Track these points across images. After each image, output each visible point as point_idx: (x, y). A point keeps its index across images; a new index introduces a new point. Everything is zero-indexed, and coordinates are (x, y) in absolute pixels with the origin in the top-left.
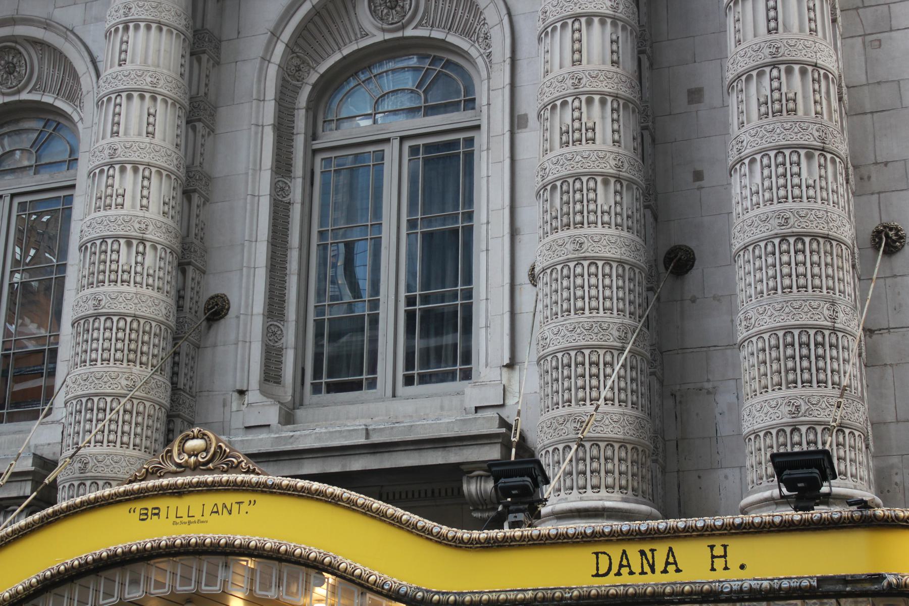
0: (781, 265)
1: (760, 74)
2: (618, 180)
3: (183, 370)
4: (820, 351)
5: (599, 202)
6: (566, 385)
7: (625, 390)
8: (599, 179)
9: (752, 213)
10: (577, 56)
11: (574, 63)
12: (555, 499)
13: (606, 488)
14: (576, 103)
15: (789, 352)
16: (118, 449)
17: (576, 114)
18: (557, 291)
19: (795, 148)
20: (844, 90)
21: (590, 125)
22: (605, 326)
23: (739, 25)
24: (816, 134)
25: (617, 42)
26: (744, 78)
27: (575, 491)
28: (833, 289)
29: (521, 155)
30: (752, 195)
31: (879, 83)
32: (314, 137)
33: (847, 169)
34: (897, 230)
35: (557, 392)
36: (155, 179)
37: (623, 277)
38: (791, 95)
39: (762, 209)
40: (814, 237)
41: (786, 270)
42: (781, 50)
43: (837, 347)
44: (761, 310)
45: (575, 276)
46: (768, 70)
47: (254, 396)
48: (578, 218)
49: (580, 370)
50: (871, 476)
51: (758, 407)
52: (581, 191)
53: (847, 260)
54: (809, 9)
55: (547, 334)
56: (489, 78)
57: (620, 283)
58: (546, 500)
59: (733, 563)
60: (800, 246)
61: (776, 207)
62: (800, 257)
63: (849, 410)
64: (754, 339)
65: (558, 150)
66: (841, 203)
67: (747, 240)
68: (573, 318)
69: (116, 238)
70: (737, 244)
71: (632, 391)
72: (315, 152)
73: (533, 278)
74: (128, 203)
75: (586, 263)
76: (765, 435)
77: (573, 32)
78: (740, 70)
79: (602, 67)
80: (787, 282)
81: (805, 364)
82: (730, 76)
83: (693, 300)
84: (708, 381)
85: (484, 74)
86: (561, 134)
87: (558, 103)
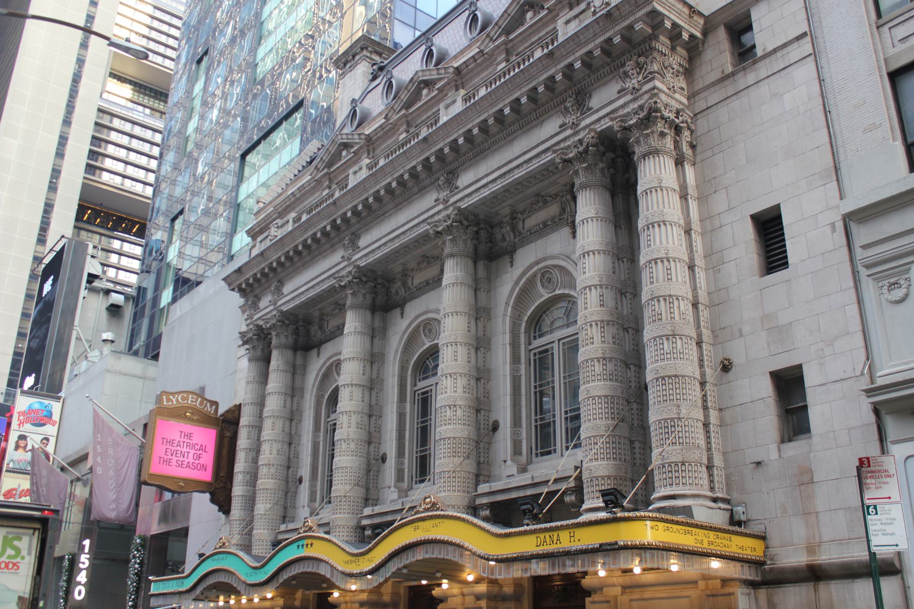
2: (604, 359)
3: (482, 455)
16: (451, 493)
19: (661, 337)
32: (530, 344)
34: (728, 360)
36: (459, 379)
40: (670, 377)
47: (509, 462)
59: (576, 538)
69: (445, 406)
72: (530, 351)
74: (449, 390)
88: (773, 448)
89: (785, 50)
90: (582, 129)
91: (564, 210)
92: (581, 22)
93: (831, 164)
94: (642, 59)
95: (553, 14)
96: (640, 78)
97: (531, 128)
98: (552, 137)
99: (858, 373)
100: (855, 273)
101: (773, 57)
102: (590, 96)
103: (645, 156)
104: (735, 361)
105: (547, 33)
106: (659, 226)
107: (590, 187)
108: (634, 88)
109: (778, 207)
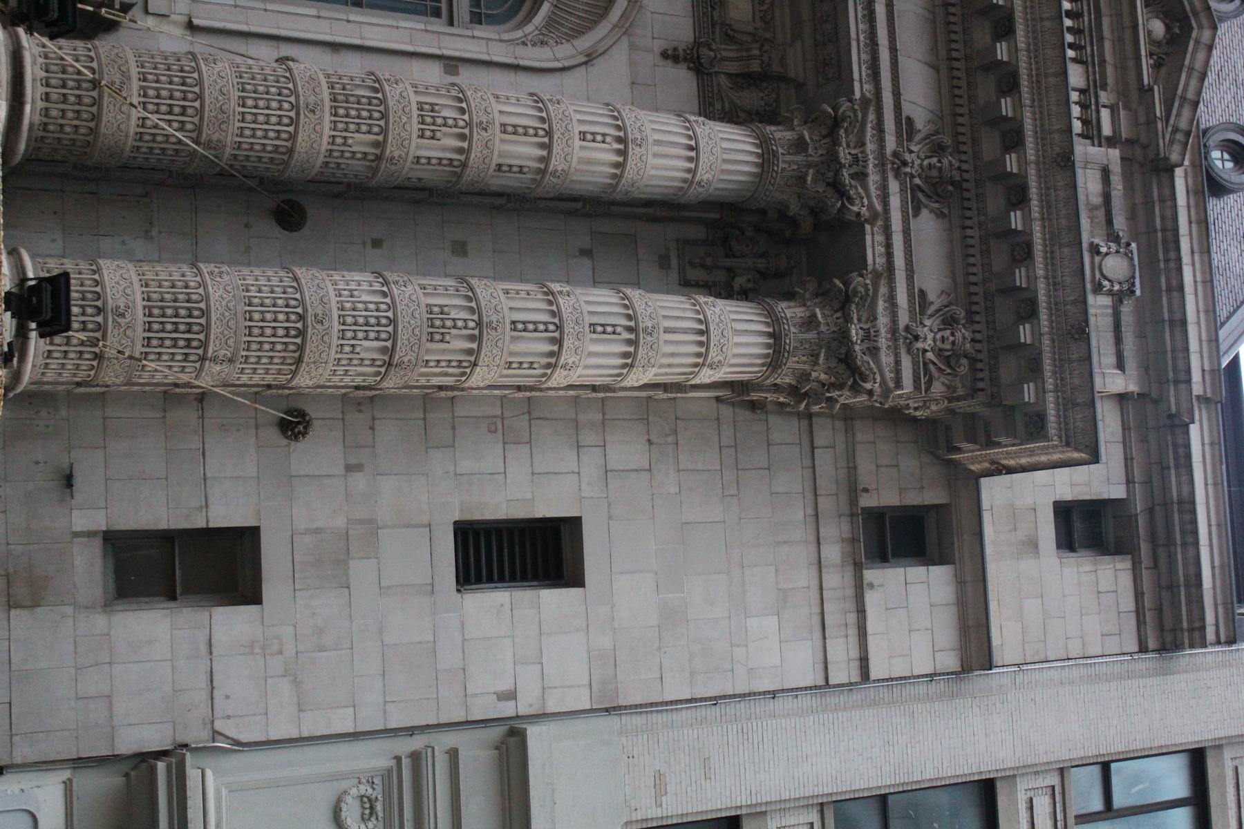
0: (275, 312)
1: (472, 310)
2: (378, 158)
4: (181, 343)
5: (356, 135)
6: (163, 78)
7: (154, 141)
8: (380, 138)
9: (330, 288)
10: (510, 129)
11: (503, 125)
12: (32, 45)
13: (47, 109)
14: (461, 123)
15: (183, 312)
17: (450, 122)
18: (265, 80)
19: (393, 337)
20: (450, 394)
21: (438, 134)
22: (224, 127)
23: (523, 295)
24: (406, 359)
25: (521, 172)
26: (470, 294)
27: (44, 74)
28: (246, 362)
29: (416, 66)
30: (351, 290)
31: (454, 428)
33: (370, 388)
34: (304, 434)
35: (155, 68)
37: (275, 151)
38: (447, 338)
39: (334, 300)
40: (301, 348)
41: (269, 316)
42: (494, 333)
43: (185, 360)
44: (228, 288)
45: (280, 101)
46: (476, 317)
48: (341, 112)
49: (177, 94)
50: (46, 387)
51: (126, 276)
52: (370, 118)
53: (275, 379)
54: (532, 363)
55: (220, 65)
56: (501, 41)
57: (269, 148)
58: (32, 34)
60: (293, 333)
61: (335, 313)
62: (281, 332)
63: (117, 367)
64: (198, 279)
65: (414, 99)
66: (335, 379)
67: (303, 281)
68: (235, 94)
70: (300, 272)
71: (151, 148)
73: (281, 60)
75: (292, 114)
76: (95, 280)
77: (535, 129)
78: (478, 291)
79: (496, 153)
80: (256, 316)
81: (169, 327)
82: (474, 282)
83: (247, 226)
84: (160, 232)
85: (506, 36)
86: (431, 104)
87: (464, 105)
88: (99, 521)
89: (853, 632)
90: (885, 179)
91: (730, 38)
92: (1095, 208)
93: (622, 703)
94: (964, 367)
95: (1134, 94)
96: (930, 355)
97: (935, 33)
98: (897, 94)
99: (219, 725)
100: (411, 731)
101: (850, 605)
102: (940, 215)
103: (774, 318)
104: (301, 446)
105: (1103, 62)
106: (626, 355)
107: (760, 176)
108: (917, 338)
109: (577, 580)
